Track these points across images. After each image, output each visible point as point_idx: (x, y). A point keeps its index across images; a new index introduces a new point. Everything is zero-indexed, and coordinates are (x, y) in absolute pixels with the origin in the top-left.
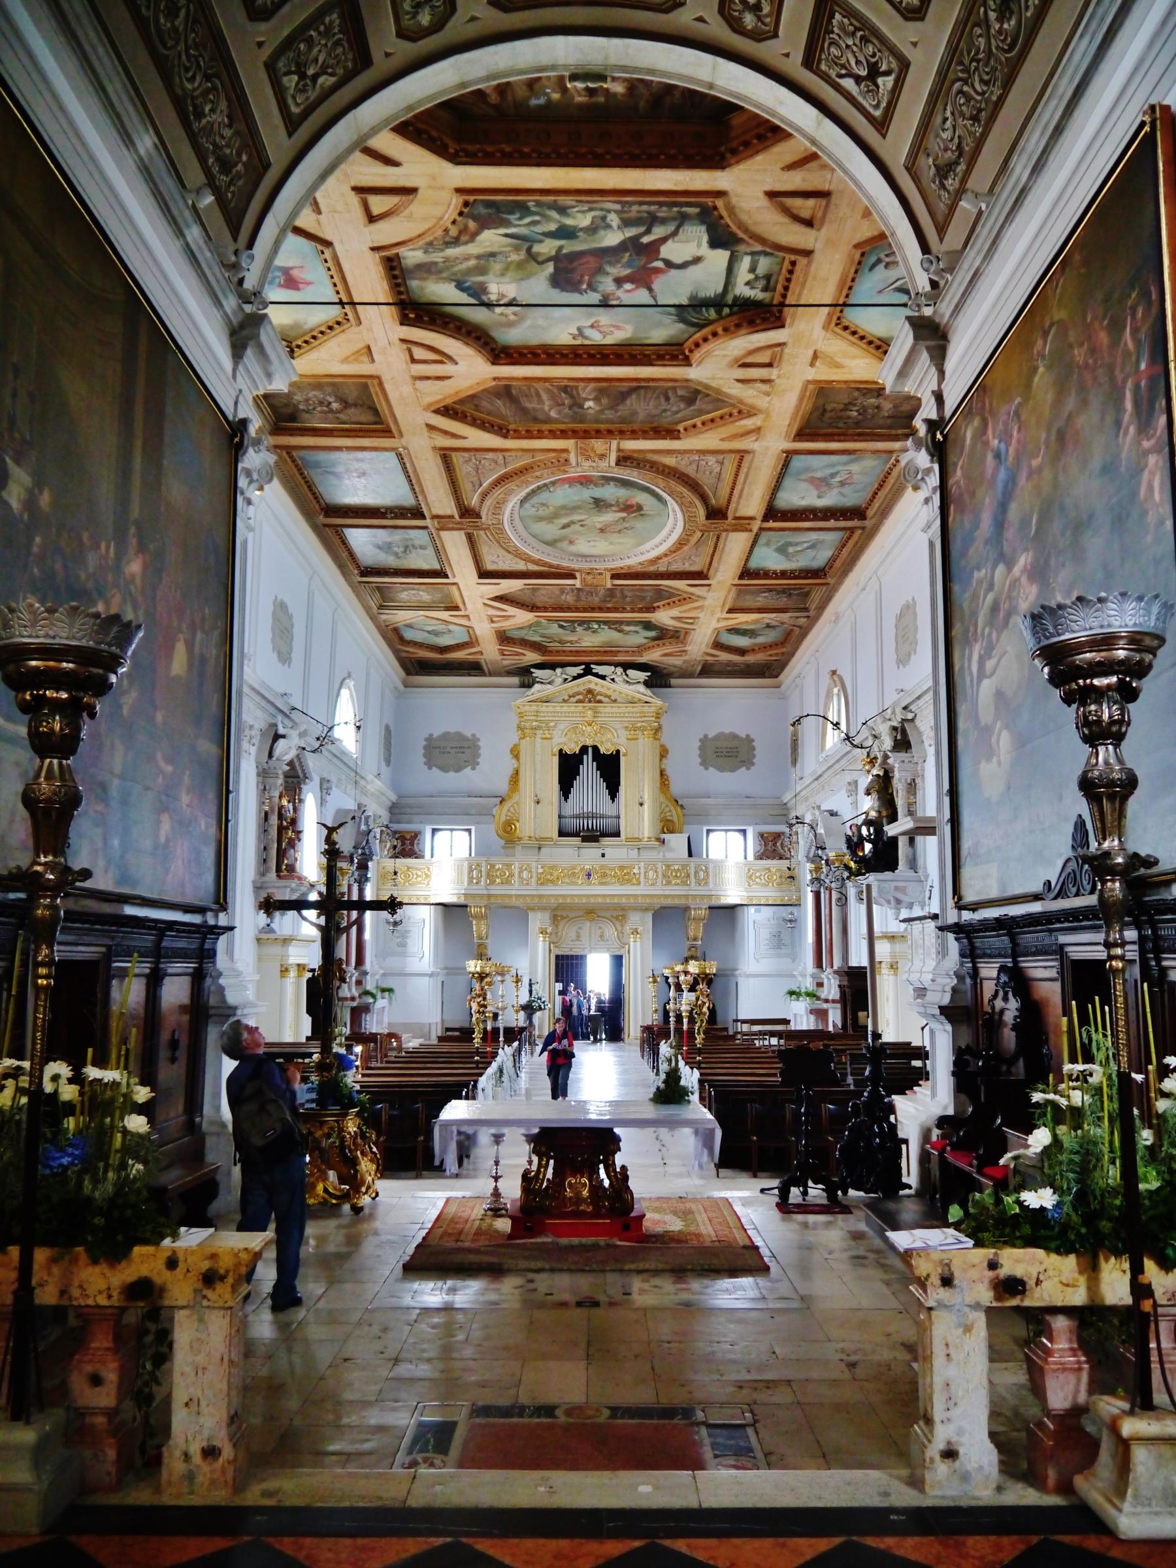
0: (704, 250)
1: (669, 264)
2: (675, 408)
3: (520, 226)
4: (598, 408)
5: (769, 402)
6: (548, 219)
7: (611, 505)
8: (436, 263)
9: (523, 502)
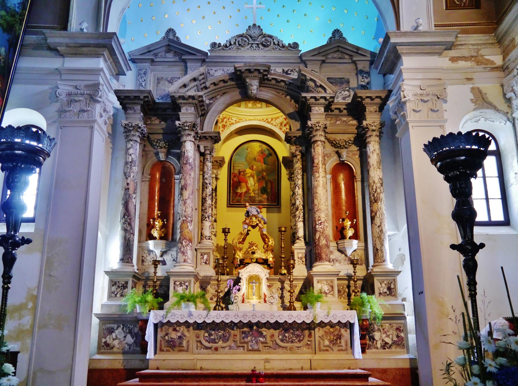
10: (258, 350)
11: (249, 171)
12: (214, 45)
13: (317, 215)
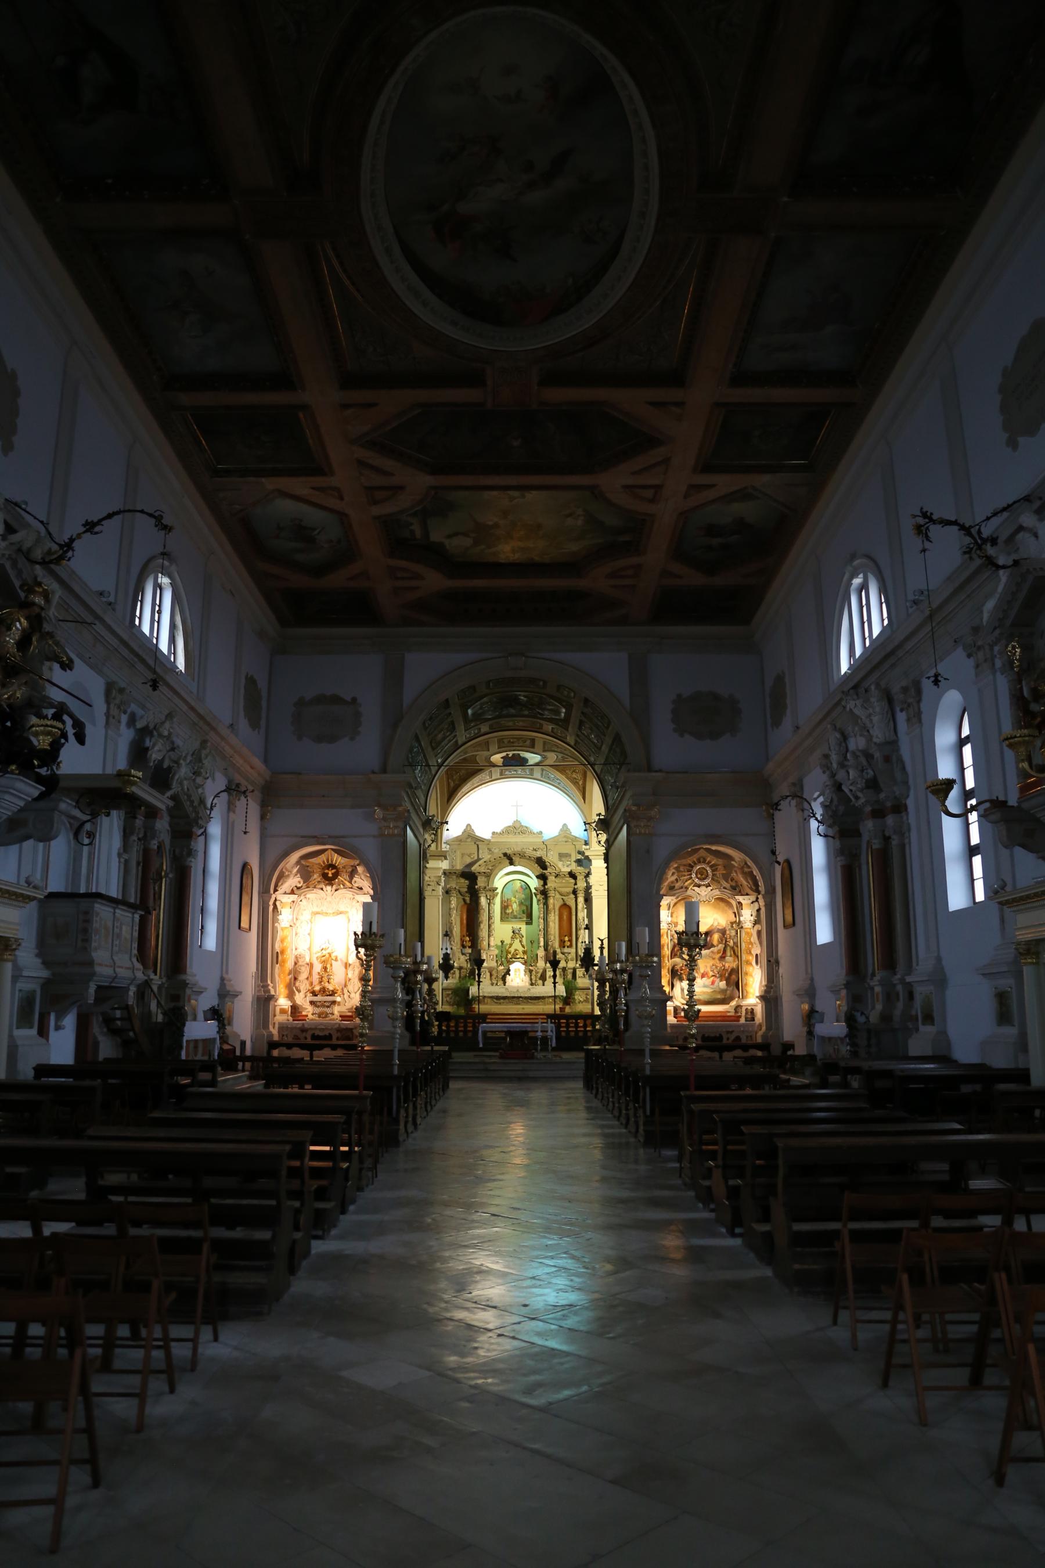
10: (519, 1004)
11: (513, 899)
12: (494, 833)
13: (549, 937)
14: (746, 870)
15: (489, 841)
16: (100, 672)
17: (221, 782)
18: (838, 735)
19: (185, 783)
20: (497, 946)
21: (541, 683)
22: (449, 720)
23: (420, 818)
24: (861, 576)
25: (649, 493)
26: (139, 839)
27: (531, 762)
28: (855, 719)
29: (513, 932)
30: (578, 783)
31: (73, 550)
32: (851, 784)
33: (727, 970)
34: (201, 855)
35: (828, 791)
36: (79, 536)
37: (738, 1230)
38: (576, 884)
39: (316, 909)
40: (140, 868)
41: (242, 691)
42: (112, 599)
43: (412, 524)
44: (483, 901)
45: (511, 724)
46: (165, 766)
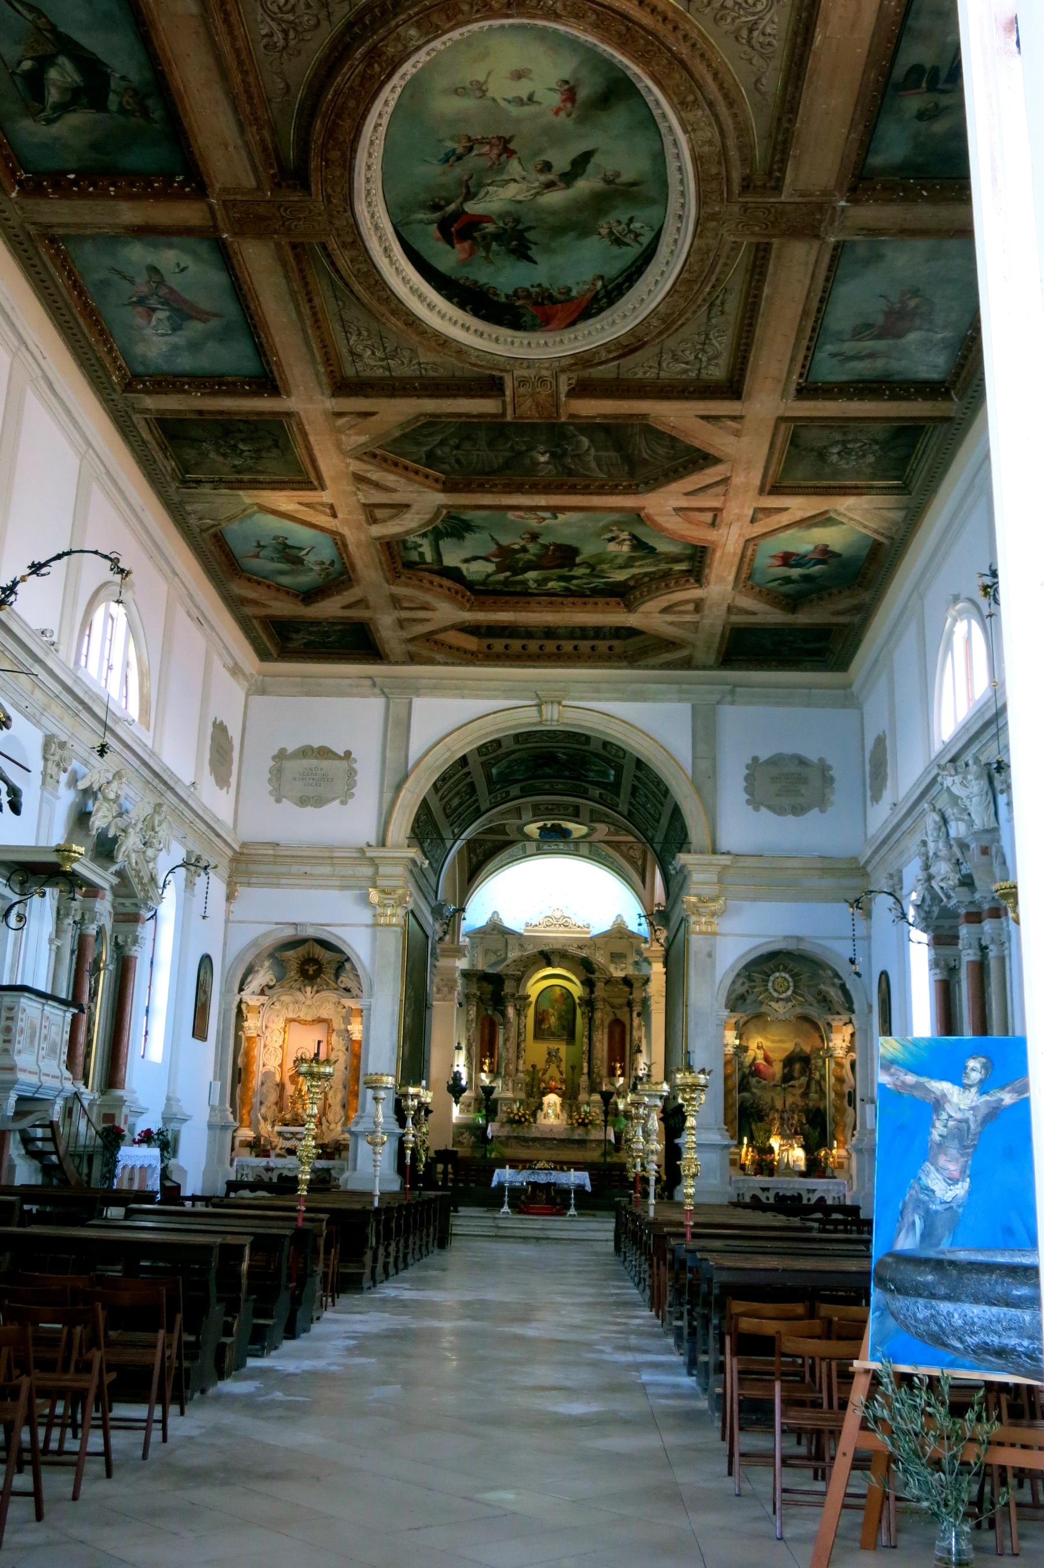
0: (464, 567)
1: (486, 559)
2: (447, 449)
3: (597, 582)
4: (534, 453)
5: (348, 465)
6: (577, 586)
7: (498, 237)
8: (667, 563)
9: (648, 255)
11: (551, 1010)
12: (527, 925)
13: (595, 1062)
14: (836, 981)
15: (521, 935)
16: (38, 724)
17: (178, 854)
18: (937, 818)
19: (133, 856)
20: (527, 1072)
21: (583, 739)
22: (468, 780)
23: (429, 903)
24: (965, 622)
25: (708, 517)
26: (75, 922)
27: (576, 835)
28: (955, 799)
29: (549, 1054)
30: (636, 863)
31: (16, 594)
32: (942, 880)
33: (811, 1111)
34: (149, 944)
35: (919, 888)
36: (23, 579)
37: (695, 1372)
38: (631, 994)
39: (291, 1015)
40: (74, 958)
41: (209, 742)
42: (55, 639)
43: (421, 546)
44: (511, 1012)
45: (547, 787)
46: (110, 835)
